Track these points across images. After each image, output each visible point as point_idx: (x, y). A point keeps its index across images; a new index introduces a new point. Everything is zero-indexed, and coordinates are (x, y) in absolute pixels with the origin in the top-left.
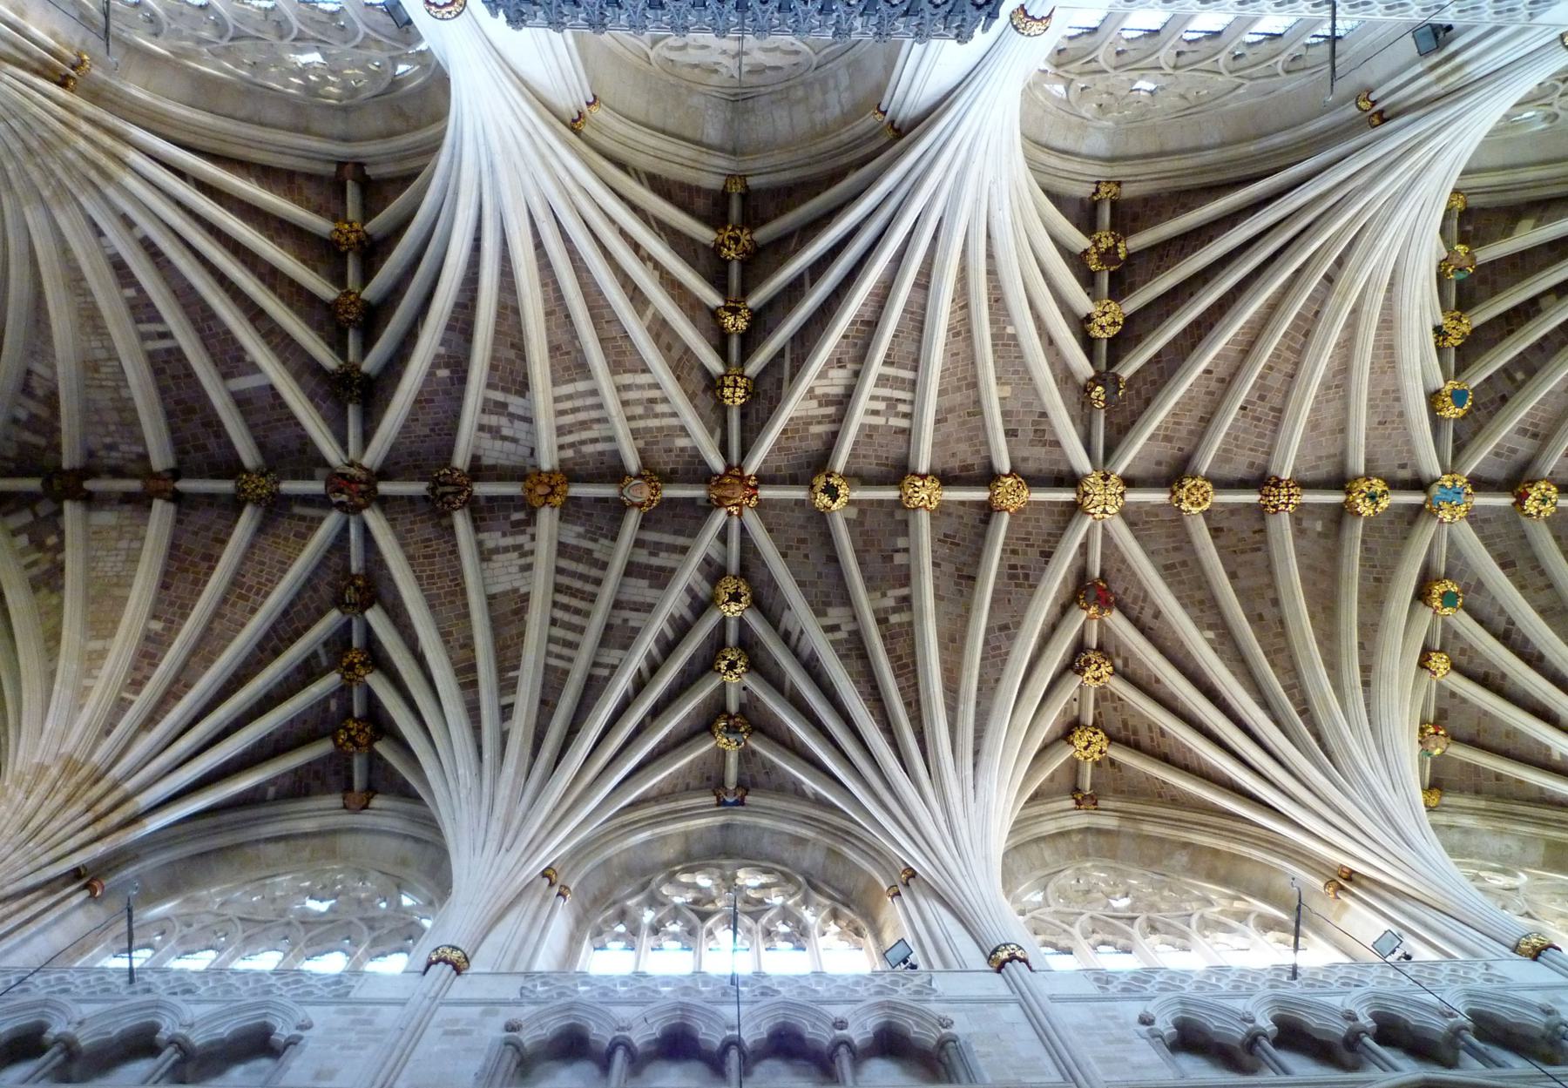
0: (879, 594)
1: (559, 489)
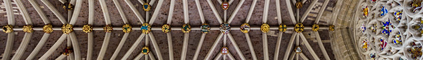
0: (14, 50)
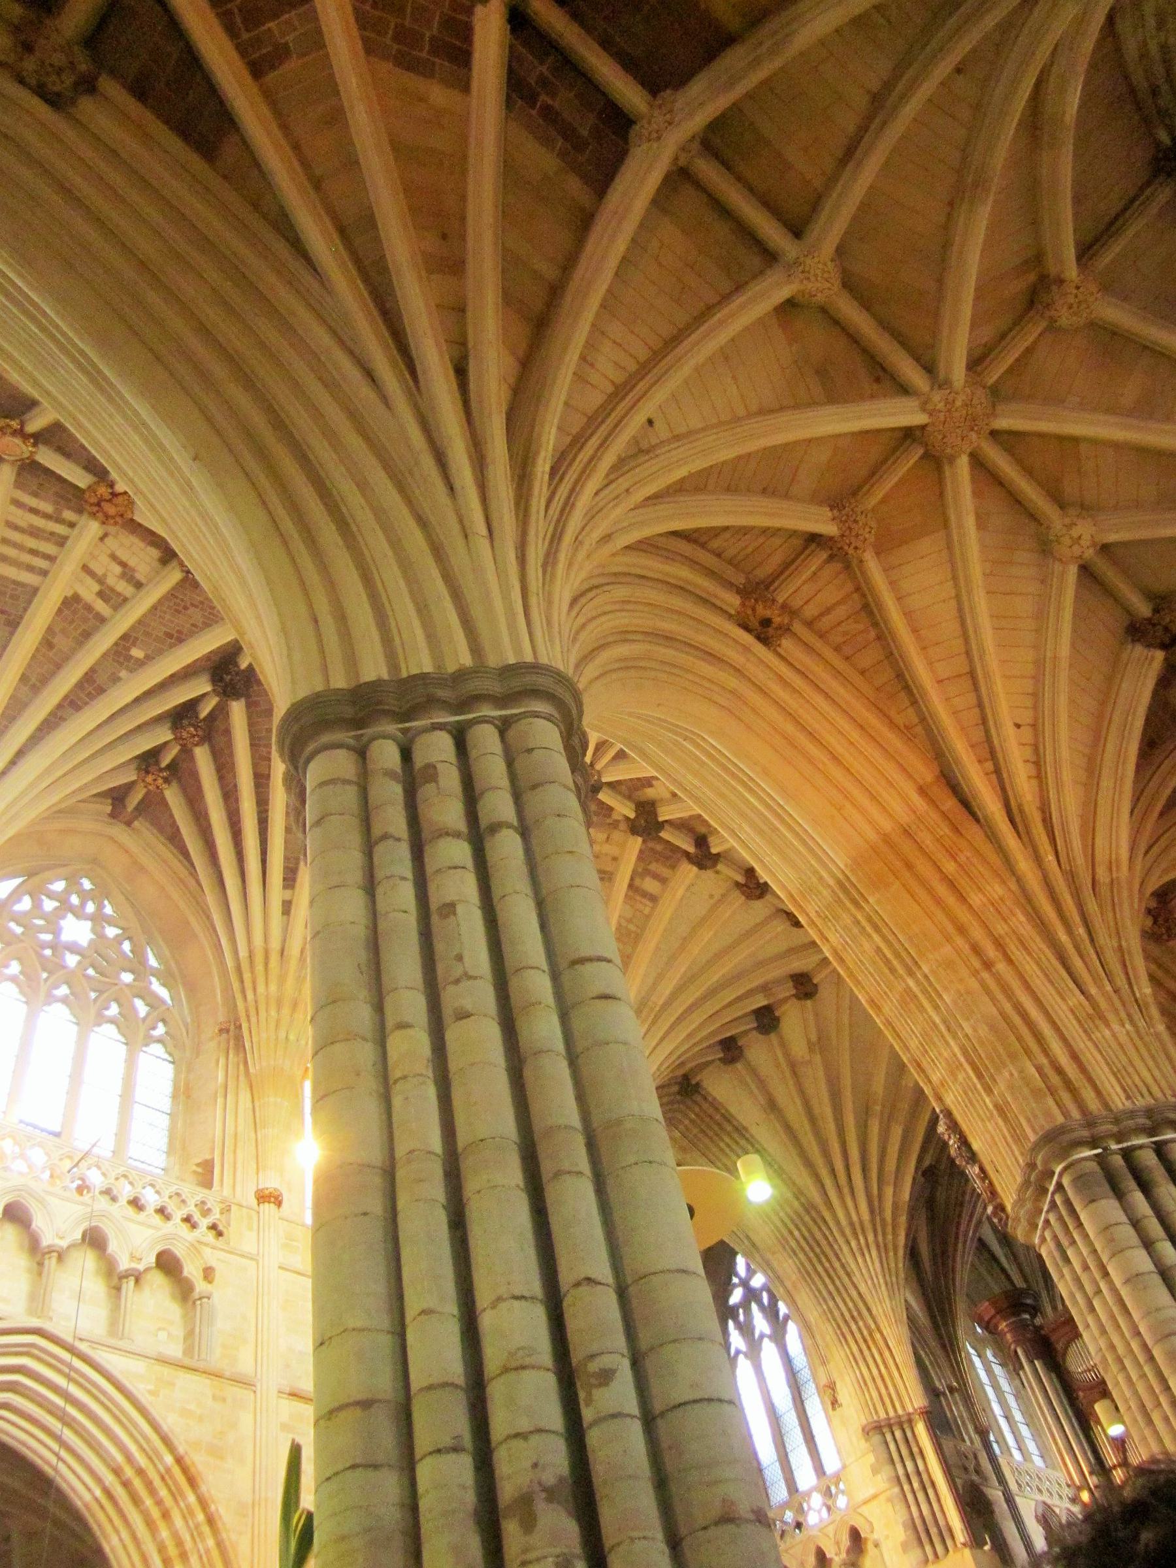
1: (94, 500)
